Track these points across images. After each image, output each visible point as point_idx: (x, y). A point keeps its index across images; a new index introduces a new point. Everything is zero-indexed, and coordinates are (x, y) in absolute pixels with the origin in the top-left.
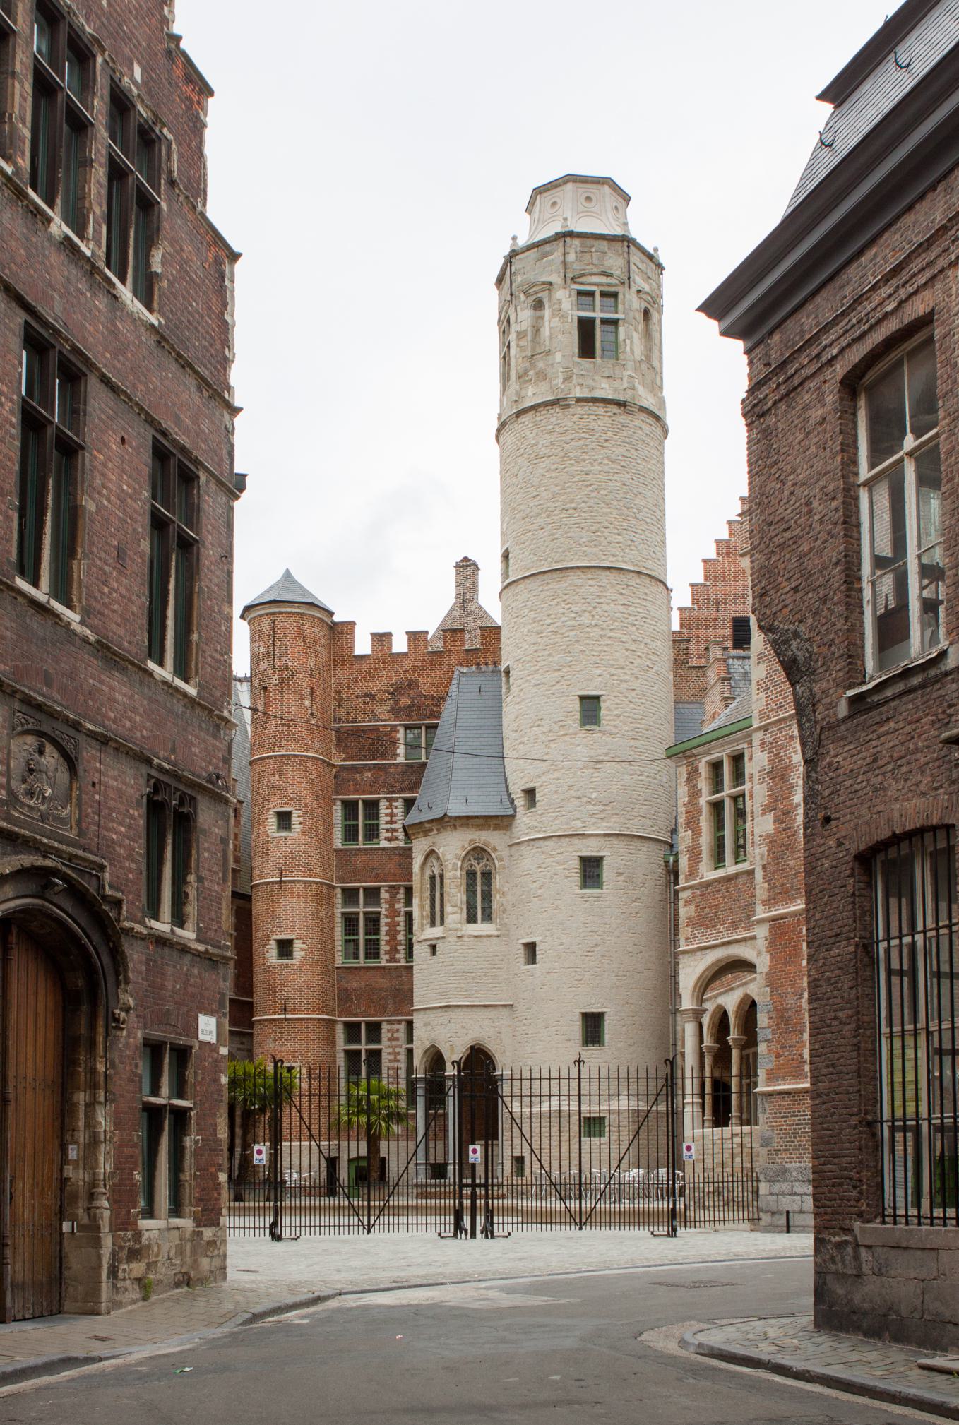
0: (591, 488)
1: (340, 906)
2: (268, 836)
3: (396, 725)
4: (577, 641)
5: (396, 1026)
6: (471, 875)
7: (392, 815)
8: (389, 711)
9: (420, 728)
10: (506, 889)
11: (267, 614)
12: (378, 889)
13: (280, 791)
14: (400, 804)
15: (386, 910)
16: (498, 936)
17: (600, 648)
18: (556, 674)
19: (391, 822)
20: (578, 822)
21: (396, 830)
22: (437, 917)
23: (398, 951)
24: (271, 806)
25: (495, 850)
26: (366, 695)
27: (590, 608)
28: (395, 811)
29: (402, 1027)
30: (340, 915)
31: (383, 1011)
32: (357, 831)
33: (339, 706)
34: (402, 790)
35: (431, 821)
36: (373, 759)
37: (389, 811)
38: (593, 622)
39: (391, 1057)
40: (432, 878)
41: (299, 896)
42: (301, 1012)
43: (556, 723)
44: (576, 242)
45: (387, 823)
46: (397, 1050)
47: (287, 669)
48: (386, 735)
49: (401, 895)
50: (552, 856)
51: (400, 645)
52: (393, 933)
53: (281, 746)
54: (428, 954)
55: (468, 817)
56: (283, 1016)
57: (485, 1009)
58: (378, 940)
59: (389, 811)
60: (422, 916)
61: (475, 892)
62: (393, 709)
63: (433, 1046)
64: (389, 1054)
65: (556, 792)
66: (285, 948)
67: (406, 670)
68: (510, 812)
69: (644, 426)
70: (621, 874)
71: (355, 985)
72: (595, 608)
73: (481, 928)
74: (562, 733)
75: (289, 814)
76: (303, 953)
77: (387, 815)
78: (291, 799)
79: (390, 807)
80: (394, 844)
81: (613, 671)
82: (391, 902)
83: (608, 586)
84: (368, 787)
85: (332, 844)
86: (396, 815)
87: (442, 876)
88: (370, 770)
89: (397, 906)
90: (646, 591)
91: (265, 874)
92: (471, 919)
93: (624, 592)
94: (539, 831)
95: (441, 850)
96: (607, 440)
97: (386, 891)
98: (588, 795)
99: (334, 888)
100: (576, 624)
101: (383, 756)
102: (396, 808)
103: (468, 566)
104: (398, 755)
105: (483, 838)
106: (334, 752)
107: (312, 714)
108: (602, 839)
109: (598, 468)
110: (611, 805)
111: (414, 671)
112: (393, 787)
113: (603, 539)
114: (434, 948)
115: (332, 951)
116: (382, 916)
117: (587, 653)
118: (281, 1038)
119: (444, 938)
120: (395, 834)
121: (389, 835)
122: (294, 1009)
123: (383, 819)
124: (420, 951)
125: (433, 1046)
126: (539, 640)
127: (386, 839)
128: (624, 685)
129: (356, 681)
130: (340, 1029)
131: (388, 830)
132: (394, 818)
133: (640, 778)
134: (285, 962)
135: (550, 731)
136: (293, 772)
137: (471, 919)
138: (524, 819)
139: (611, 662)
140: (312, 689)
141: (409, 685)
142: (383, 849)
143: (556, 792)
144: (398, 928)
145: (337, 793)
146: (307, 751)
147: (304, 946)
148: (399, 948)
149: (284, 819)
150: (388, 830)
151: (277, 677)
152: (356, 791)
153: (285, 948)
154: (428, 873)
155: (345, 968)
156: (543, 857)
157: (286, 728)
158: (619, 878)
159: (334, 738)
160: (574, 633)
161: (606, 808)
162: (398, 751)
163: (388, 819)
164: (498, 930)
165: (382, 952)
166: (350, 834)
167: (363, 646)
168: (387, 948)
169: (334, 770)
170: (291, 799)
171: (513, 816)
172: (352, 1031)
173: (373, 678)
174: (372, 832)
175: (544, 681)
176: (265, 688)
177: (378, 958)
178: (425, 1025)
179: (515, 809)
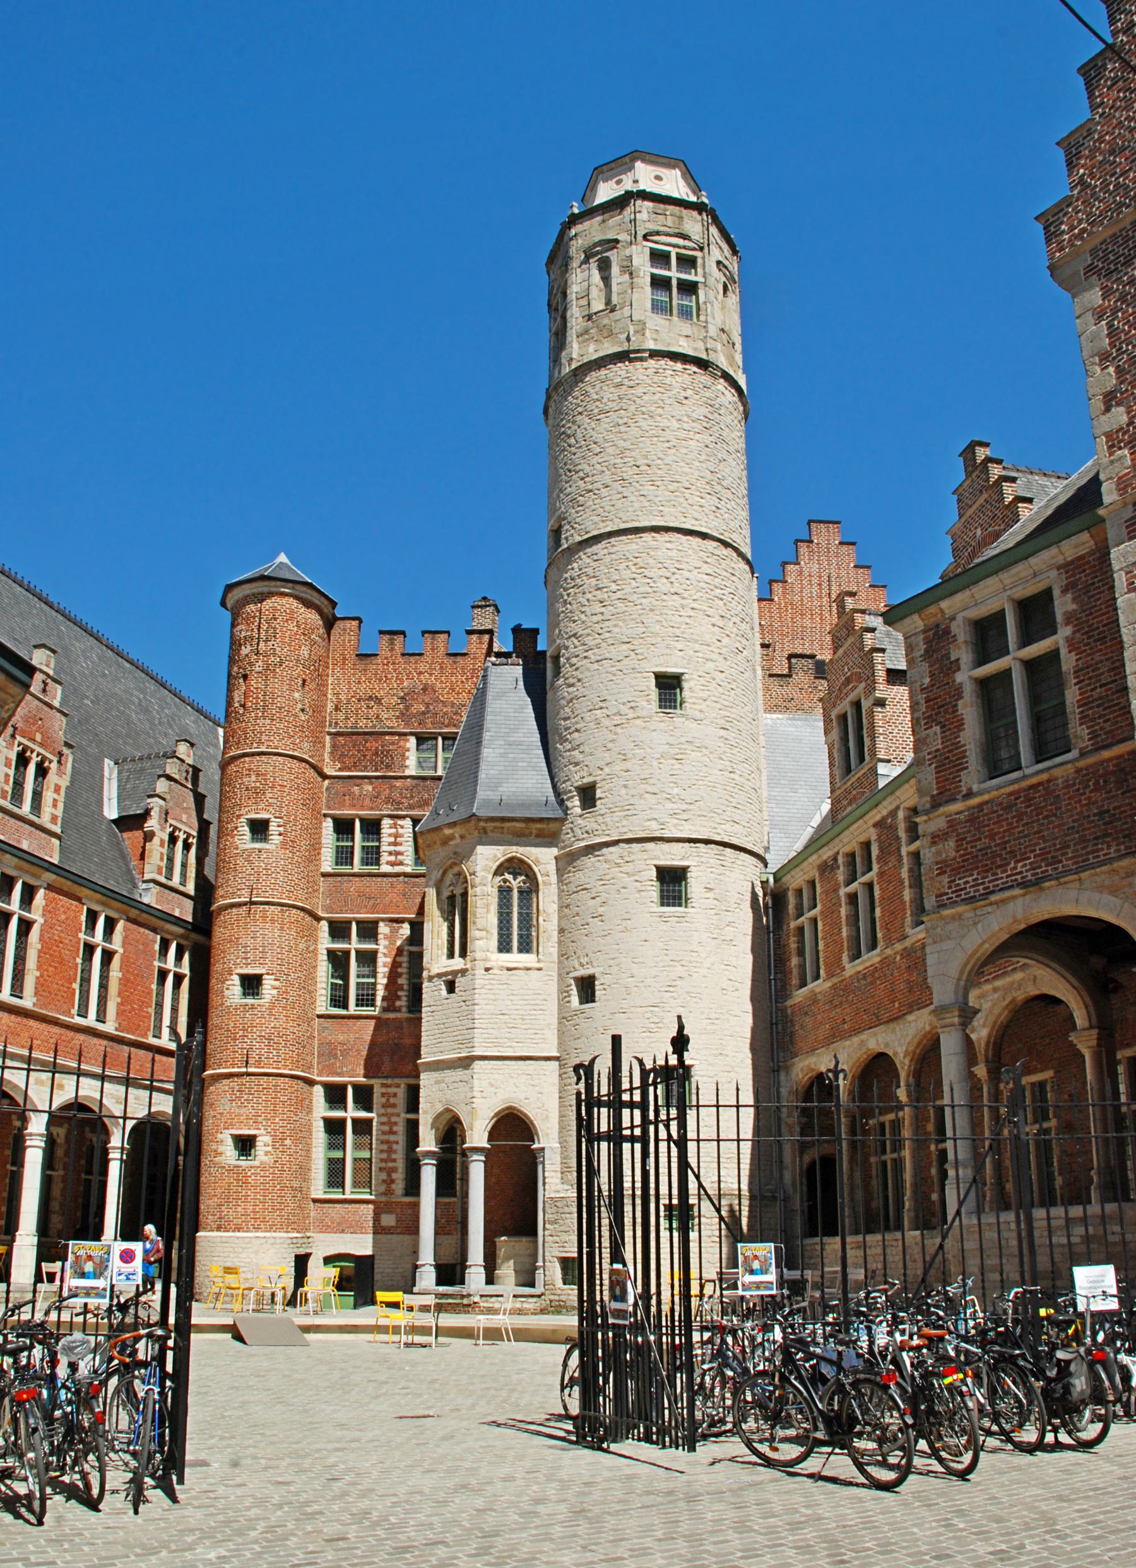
0: (667, 445)
1: (325, 941)
2: (237, 849)
3: (405, 734)
4: (652, 610)
6: (504, 892)
7: (396, 836)
8: (398, 717)
9: (436, 739)
12: (375, 923)
14: (408, 823)
15: (385, 947)
16: (540, 969)
17: (680, 619)
18: (625, 647)
19: (395, 844)
22: (460, 946)
23: (399, 998)
24: (243, 811)
27: (668, 575)
28: (401, 831)
29: (401, 1092)
30: (325, 952)
32: (352, 853)
33: (337, 709)
34: (411, 807)
35: (453, 825)
36: (376, 770)
37: (393, 831)
38: (673, 591)
41: (273, 921)
43: (624, 704)
44: (649, 205)
45: (390, 844)
48: (393, 744)
50: (618, 865)
54: (444, 992)
55: (503, 819)
59: (393, 831)
61: (509, 914)
62: (403, 714)
63: (448, 1110)
65: (625, 786)
66: (252, 984)
67: (421, 673)
68: (559, 814)
69: (726, 392)
71: (341, 1038)
73: (515, 958)
74: (631, 716)
76: (275, 992)
77: (390, 835)
78: (270, 805)
79: (395, 826)
81: (697, 647)
83: (690, 552)
84: (367, 802)
85: (318, 866)
87: (465, 894)
90: (733, 565)
92: (504, 946)
93: (709, 560)
96: (686, 398)
98: (668, 791)
99: (318, 919)
100: (650, 590)
102: (402, 827)
103: (486, 606)
106: (327, 760)
109: (675, 424)
111: (431, 675)
112: (399, 803)
113: (682, 500)
116: (380, 955)
117: (664, 623)
120: (400, 857)
121: (393, 858)
122: (259, 1061)
123: (386, 839)
124: (433, 992)
125: (448, 1110)
126: (603, 610)
127: (388, 863)
128: (710, 664)
129: (359, 683)
131: (390, 853)
132: (399, 840)
133: (732, 775)
135: (614, 715)
136: (274, 772)
137: (504, 946)
139: (695, 637)
140: (304, 681)
141: (425, 689)
142: (385, 875)
144: (399, 970)
145: (329, 808)
148: (399, 993)
150: (390, 853)
152: (354, 806)
153: (252, 984)
157: (269, 722)
158: (708, 895)
159: (328, 745)
160: (649, 600)
161: (691, 807)
162: (407, 763)
163: (392, 839)
166: (344, 856)
170: (270, 805)
171: (562, 821)
173: (380, 680)
174: (372, 856)
175: (607, 655)
179: (566, 810)
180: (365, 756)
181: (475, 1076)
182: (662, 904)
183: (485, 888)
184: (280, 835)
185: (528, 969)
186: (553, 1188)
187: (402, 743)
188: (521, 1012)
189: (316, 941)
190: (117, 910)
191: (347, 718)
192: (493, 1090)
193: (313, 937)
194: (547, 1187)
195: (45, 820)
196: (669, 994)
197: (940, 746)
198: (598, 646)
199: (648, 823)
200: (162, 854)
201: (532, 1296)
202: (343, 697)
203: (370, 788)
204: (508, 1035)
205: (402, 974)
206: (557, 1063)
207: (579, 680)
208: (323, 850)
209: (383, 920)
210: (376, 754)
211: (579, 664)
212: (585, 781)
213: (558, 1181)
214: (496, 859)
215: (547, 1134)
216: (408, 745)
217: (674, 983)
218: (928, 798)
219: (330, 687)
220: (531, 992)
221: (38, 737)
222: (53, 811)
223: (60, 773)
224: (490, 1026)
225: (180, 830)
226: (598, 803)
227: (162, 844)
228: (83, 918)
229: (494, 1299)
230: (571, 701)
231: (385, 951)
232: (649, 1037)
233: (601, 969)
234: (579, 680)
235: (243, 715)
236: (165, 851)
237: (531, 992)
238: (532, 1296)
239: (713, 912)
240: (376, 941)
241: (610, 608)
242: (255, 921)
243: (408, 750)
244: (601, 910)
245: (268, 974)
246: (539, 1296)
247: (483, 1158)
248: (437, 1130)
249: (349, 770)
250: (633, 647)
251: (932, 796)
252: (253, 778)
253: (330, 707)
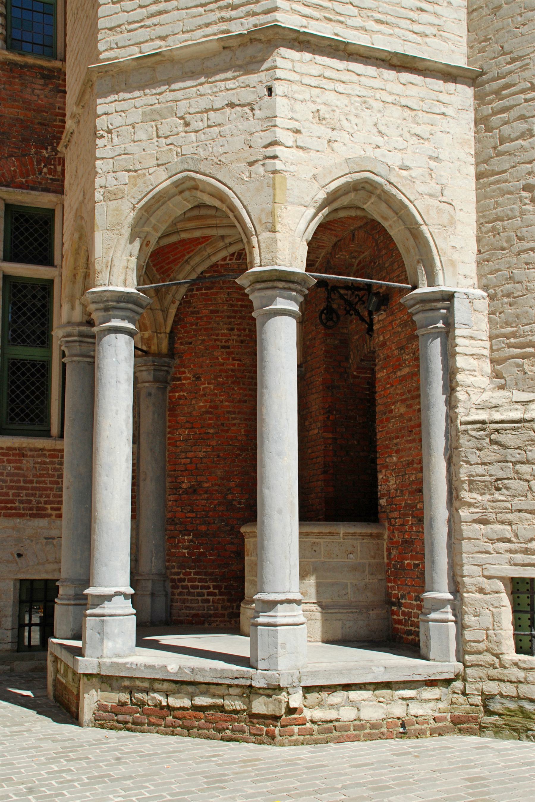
181: (279, 88)
186: (476, 399)
192: (324, 131)
194: (461, 394)
201: (431, 683)
206: (469, 92)
213: (484, 382)
215: (453, 263)
229: (338, 697)
238: (431, 683)
246: (447, 682)
247: (295, 307)
248: (145, 244)
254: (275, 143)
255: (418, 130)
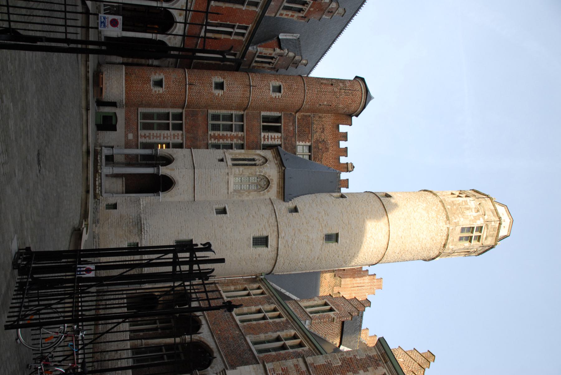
1: (235, 113)
2: (270, 81)
5: (180, 138)
7: (274, 139)
10: (250, 197)
11: (361, 88)
12: (243, 131)
13: (290, 88)
15: (234, 135)
16: (228, 193)
18: (347, 222)
19: (271, 138)
20: (284, 235)
21: (268, 140)
23: (215, 140)
25: (268, 191)
26: (323, 129)
28: (276, 140)
30: (231, 113)
31: (188, 132)
33: (320, 117)
34: (285, 144)
36: (298, 131)
37: (276, 137)
39: (166, 135)
40: (253, 160)
41: (243, 94)
42: (189, 92)
43: (327, 222)
45: (271, 136)
46: (169, 138)
47: (340, 95)
48: (307, 137)
49: (240, 142)
51: (343, 144)
52: (223, 137)
53: (309, 90)
56: (187, 83)
57: (193, 187)
58: (220, 130)
59: (276, 137)
60: (236, 154)
62: (318, 141)
63: (174, 159)
64: (167, 134)
65: (297, 223)
66: (220, 86)
67: (333, 147)
70: (259, 255)
72: (373, 239)
74: (323, 225)
75: (280, 92)
76: (217, 94)
77: (275, 136)
79: (278, 138)
80: (262, 139)
82: (237, 137)
84: (287, 128)
86: (274, 141)
87: (255, 165)
88: (293, 129)
89: (235, 140)
91: (255, 79)
94: (279, 215)
95: (268, 165)
97: (242, 135)
101: (299, 136)
102: (278, 141)
104: (299, 142)
105: (273, 185)
107: (320, 105)
108: (276, 246)
110: (291, 250)
111: (332, 150)
112: (286, 139)
114: (222, 160)
115: (216, 108)
116: (231, 133)
118: (176, 81)
119: (227, 166)
120: (266, 140)
121: (266, 137)
124: (219, 153)
127: (264, 136)
129: (329, 125)
130: (179, 111)
131: (268, 136)
132: (273, 140)
134: (213, 85)
135: (323, 219)
136: (298, 95)
138: (283, 207)
140: (331, 106)
141: (326, 148)
142: (260, 134)
143: (297, 223)
144: (225, 140)
145: (284, 115)
146: (306, 102)
147: (220, 95)
148: (216, 140)
149: (278, 89)
150: (268, 136)
151: (337, 90)
152: (285, 123)
154: (256, 157)
155: (208, 114)
156: (267, 218)
157: (316, 92)
161: (290, 248)
163: (273, 137)
164: (231, 193)
165: (215, 132)
167: (343, 128)
168: (216, 135)
169: (293, 113)
172: (179, 117)
176: (332, 85)
177: (212, 130)
178: (184, 155)
180: (303, 127)
182: (253, 238)
183: (258, 172)
184: (275, 97)
185: (228, 189)
187: (308, 140)
188: (212, 186)
189: (235, 110)
190: (247, 38)
191: (316, 121)
193: (238, 108)
195: (281, 11)
196: (220, 242)
197: (333, 365)
198: (347, 212)
199: (284, 232)
200: (266, 54)
202: (324, 119)
203: (291, 129)
204: (203, 181)
205: (224, 141)
207: (335, 206)
208: (269, 112)
209: (244, 134)
210: (304, 131)
211: (340, 206)
212: (299, 209)
214: (269, 176)
216: (307, 143)
217: (224, 244)
218: (313, 362)
219: (327, 115)
220: (219, 190)
221: (312, 9)
222: (284, 14)
223: (298, 17)
224: (206, 175)
225: (275, 61)
226: (291, 214)
227: (270, 54)
228: (244, 25)
230: (327, 203)
231: (232, 135)
232: (203, 235)
233: (229, 216)
234: (335, 206)
235: (318, 84)
236: (268, 55)
237: (219, 190)
239: (251, 257)
240: (236, 131)
241: (361, 216)
242: (244, 88)
243: (305, 143)
244: (251, 216)
245: (224, 92)
249: (298, 122)
250: (347, 225)
251: (313, 364)
252: (296, 87)
253: (320, 115)
254: (179, 169)
255: (185, 191)
